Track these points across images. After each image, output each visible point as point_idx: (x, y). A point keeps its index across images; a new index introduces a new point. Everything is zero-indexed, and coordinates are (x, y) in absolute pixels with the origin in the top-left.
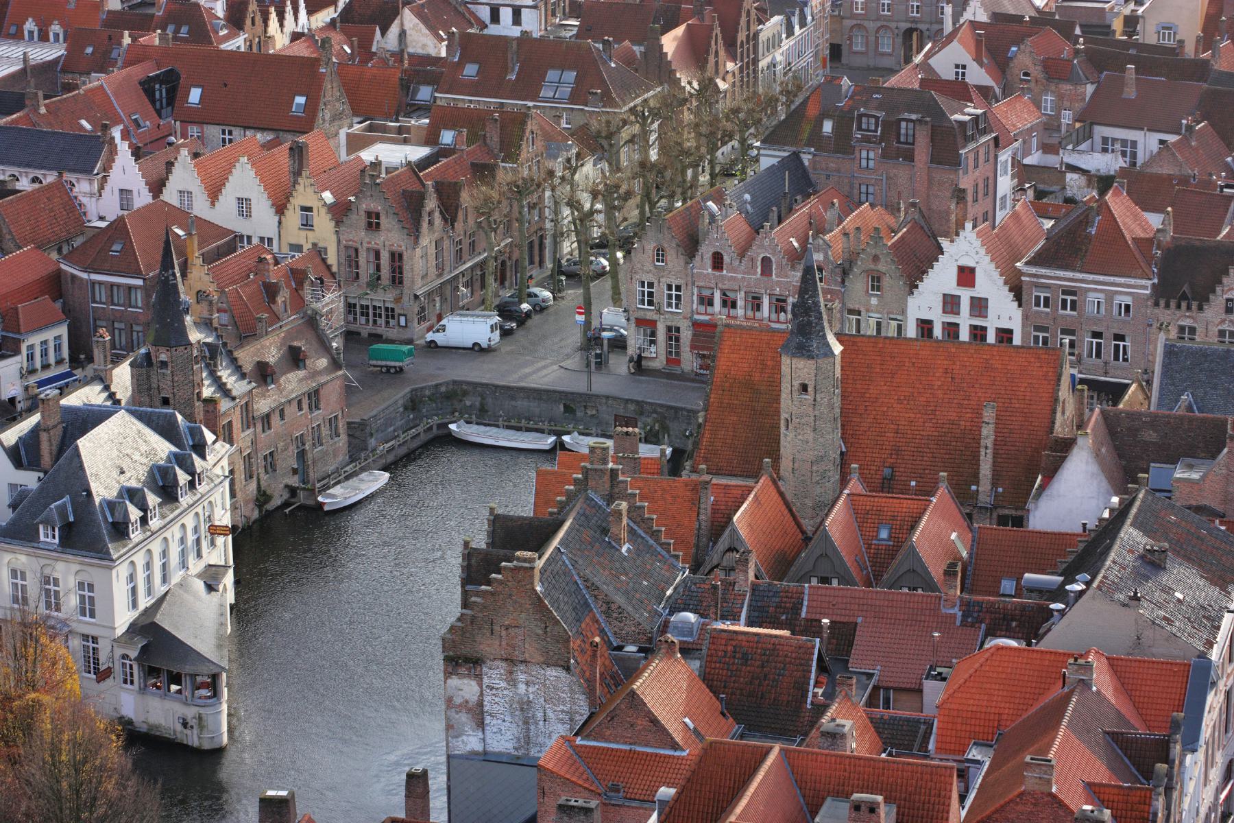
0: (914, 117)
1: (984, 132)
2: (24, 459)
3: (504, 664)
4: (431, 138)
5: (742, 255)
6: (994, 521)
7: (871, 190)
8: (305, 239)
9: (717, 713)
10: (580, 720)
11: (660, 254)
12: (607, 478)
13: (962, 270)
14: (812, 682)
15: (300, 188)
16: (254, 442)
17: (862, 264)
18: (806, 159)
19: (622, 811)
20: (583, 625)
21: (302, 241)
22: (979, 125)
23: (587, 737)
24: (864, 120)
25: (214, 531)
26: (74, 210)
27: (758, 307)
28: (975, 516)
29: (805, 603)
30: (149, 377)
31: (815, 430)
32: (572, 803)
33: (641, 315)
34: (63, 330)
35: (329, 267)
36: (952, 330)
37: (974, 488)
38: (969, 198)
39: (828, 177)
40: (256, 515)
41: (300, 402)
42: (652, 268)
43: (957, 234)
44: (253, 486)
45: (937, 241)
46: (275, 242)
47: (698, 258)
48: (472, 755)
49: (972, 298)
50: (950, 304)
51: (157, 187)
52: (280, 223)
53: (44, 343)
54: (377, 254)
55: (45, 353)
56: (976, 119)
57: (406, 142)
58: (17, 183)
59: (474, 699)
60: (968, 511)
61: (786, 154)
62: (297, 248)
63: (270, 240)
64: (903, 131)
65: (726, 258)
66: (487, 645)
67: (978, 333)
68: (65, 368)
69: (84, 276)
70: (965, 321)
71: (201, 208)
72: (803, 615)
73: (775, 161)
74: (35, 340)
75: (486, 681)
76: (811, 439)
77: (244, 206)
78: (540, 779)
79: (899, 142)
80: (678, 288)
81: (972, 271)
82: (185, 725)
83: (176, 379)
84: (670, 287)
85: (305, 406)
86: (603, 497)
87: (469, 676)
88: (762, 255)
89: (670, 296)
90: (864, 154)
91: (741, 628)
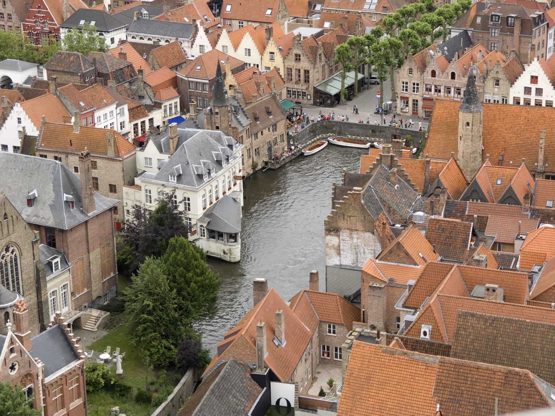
0: (514, 15)
1: (543, 22)
2: (164, 151)
3: (348, 231)
4: (321, 25)
5: (443, 72)
6: (544, 177)
7: (496, 45)
8: (272, 65)
9: (432, 251)
10: (378, 253)
11: (411, 71)
12: (389, 159)
13: (532, 77)
14: (470, 240)
15: (269, 45)
16: (251, 144)
17: (492, 74)
18: (470, 33)
19: (394, 289)
20: (379, 216)
21: (270, 66)
22: (541, 19)
23: (380, 260)
24: (494, 17)
25: (236, 178)
26: (182, 53)
27: (449, 92)
28: (536, 176)
29: (467, 209)
30: (211, 118)
31: (472, 141)
32: (375, 285)
33: (403, 95)
34: (178, 100)
35: (281, 76)
36: (527, 103)
37: (536, 164)
38: (536, 48)
39: (478, 40)
40: (251, 172)
41: (269, 128)
42: (407, 77)
43: (531, 63)
44: (251, 161)
45: (522, 66)
46: (259, 66)
47: (425, 73)
48: (335, 266)
49: (536, 89)
50: (528, 90)
51: (214, 43)
52: (261, 59)
53: (171, 104)
54: (299, 71)
55: (171, 109)
56: (539, 16)
57: (311, 26)
58: (160, 42)
59: (336, 244)
60: (533, 173)
61: (462, 31)
62: (268, 68)
63: (258, 66)
64: (509, 22)
65: (437, 73)
66: (342, 224)
67: (538, 104)
68: (179, 115)
69: (186, 79)
70: (533, 98)
71: (231, 52)
72: (467, 213)
73: (457, 34)
74: (167, 103)
75: (341, 237)
76: (470, 145)
77: (248, 52)
78: (362, 276)
79: (508, 26)
80: (418, 84)
81: (537, 77)
82: (224, 253)
83: (221, 119)
84: (414, 84)
85: (271, 129)
86: (388, 166)
87: (335, 235)
88: (451, 72)
89: (414, 88)
90: (493, 31)
91: (442, 217)
